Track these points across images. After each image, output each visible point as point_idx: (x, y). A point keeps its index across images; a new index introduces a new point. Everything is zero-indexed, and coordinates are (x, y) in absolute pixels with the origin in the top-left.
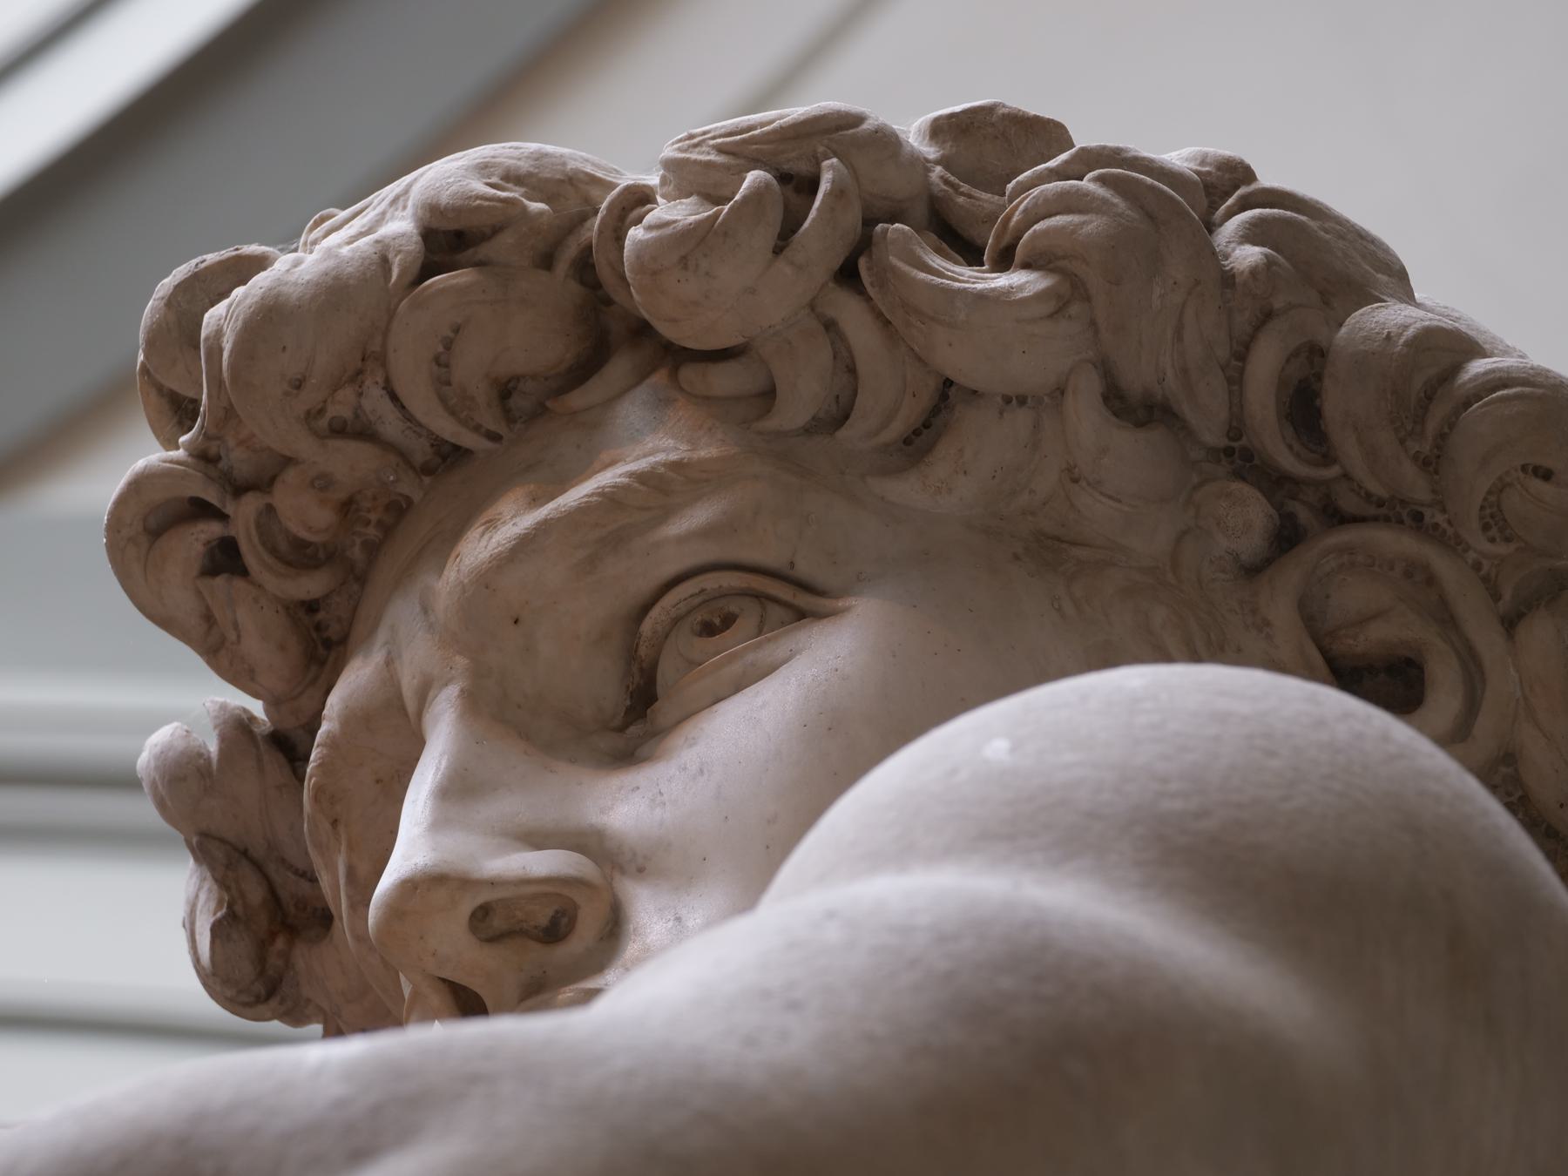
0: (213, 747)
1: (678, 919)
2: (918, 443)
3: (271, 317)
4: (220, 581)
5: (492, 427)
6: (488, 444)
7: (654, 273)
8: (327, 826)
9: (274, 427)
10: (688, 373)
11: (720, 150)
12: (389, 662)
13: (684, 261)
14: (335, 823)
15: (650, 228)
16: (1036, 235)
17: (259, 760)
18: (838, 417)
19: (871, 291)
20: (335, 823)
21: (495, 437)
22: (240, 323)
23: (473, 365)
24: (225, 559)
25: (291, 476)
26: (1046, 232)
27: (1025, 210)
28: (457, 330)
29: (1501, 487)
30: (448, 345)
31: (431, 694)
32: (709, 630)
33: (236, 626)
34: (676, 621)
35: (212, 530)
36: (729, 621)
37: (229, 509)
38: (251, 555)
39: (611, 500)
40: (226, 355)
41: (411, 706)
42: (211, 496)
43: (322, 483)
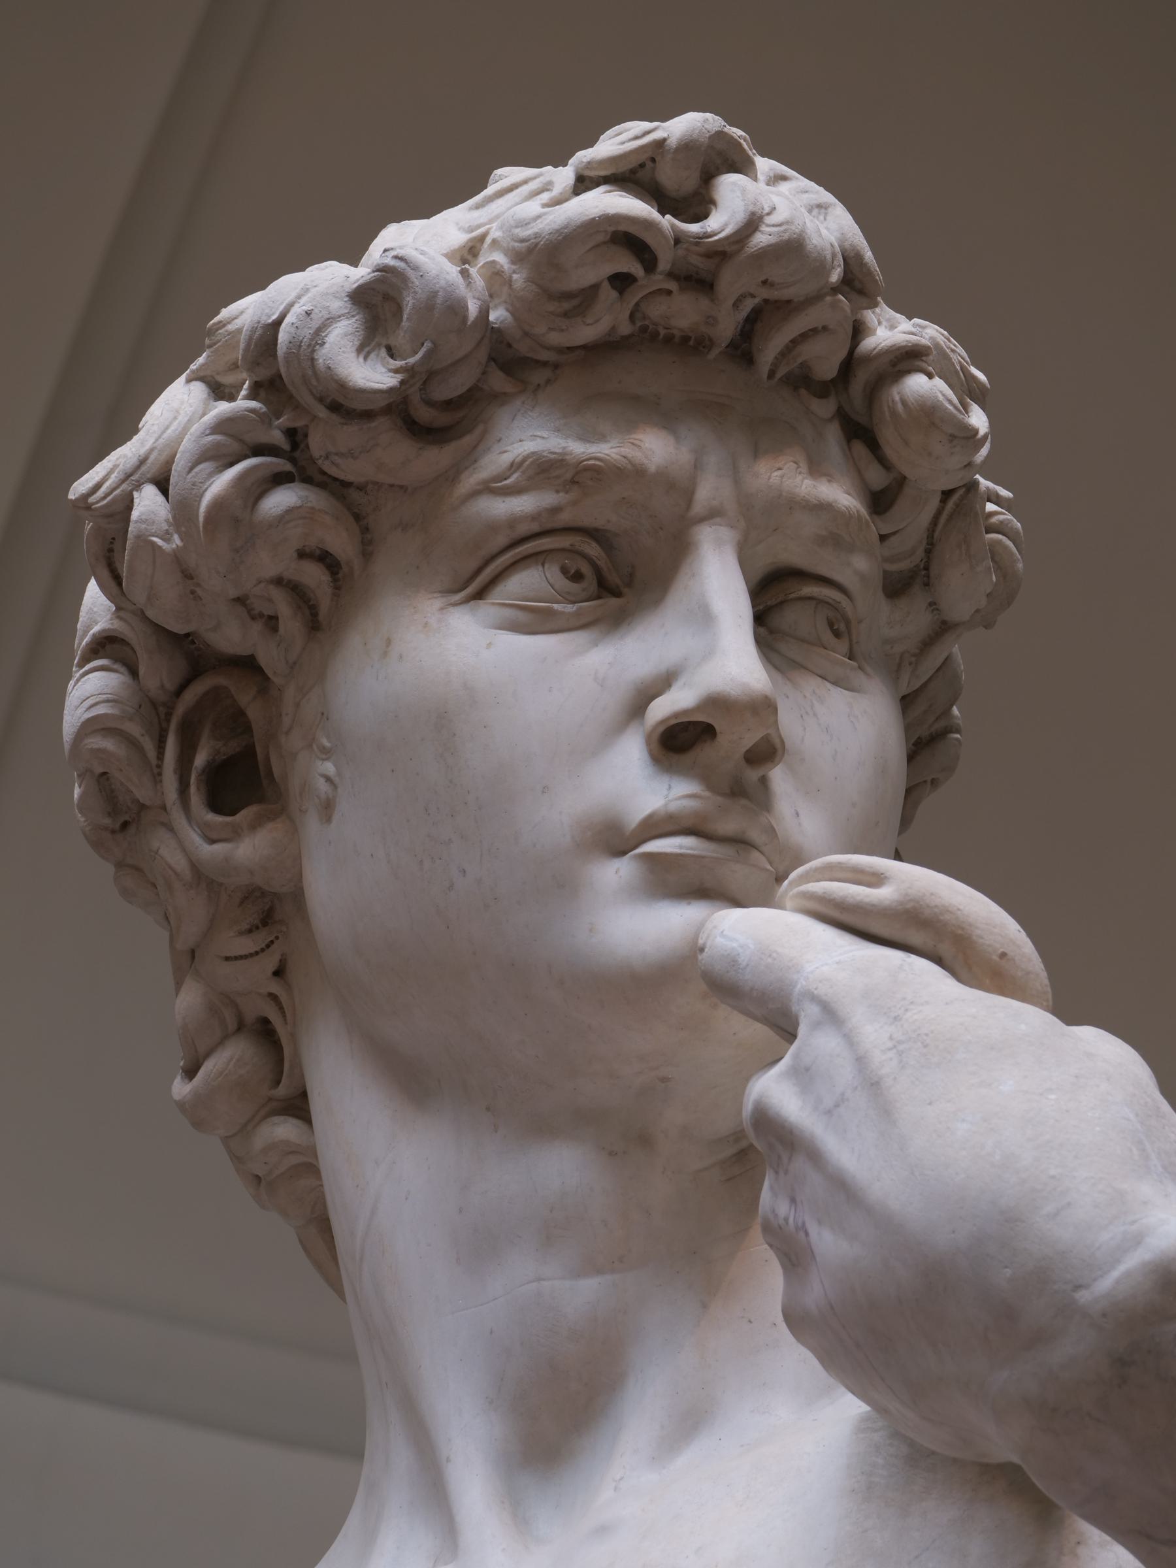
0: (473, 308)
1: (798, 814)
2: (896, 587)
3: (793, 248)
4: (614, 294)
5: (780, 374)
6: (765, 376)
7: (933, 424)
8: (569, 476)
9: (732, 282)
10: (859, 448)
11: (962, 367)
12: (695, 467)
13: (953, 437)
14: (573, 482)
15: (950, 402)
16: (1000, 542)
17: (482, 339)
18: (883, 538)
19: (950, 504)
20: (573, 482)
21: (771, 374)
22: (786, 236)
23: (810, 351)
24: (621, 281)
25: (704, 302)
26: (1006, 547)
27: (1001, 522)
28: (825, 328)
29: (925, 782)
30: (814, 331)
31: (718, 520)
32: (831, 624)
33: (597, 321)
34: (810, 598)
35: (636, 269)
36: (837, 634)
37: (658, 277)
38: (634, 296)
39: (845, 517)
40: (762, 239)
41: (698, 508)
42: (663, 265)
43: (711, 321)
